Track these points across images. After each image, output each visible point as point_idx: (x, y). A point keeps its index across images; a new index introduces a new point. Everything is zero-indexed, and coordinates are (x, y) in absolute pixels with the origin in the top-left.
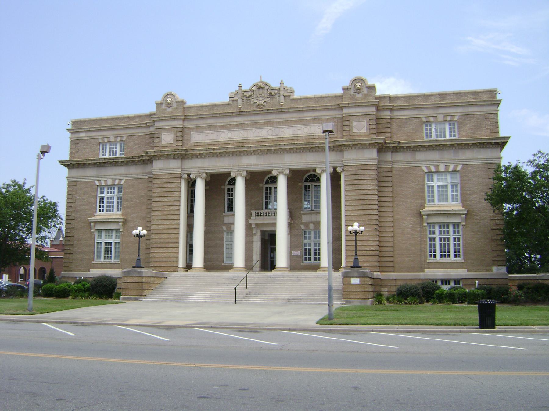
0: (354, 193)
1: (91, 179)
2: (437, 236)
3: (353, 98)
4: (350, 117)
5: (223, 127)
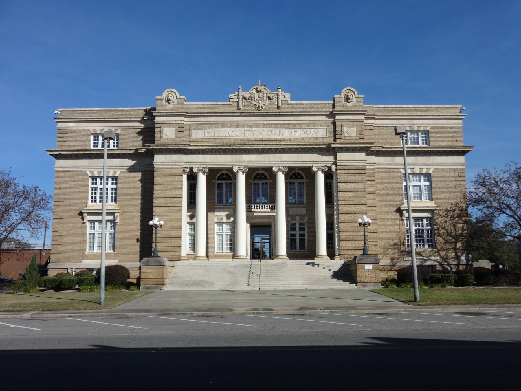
0: (346, 190)
1: (83, 170)
2: (414, 229)
3: (344, 106)
4: (342, 123)
5: (224, 126)
